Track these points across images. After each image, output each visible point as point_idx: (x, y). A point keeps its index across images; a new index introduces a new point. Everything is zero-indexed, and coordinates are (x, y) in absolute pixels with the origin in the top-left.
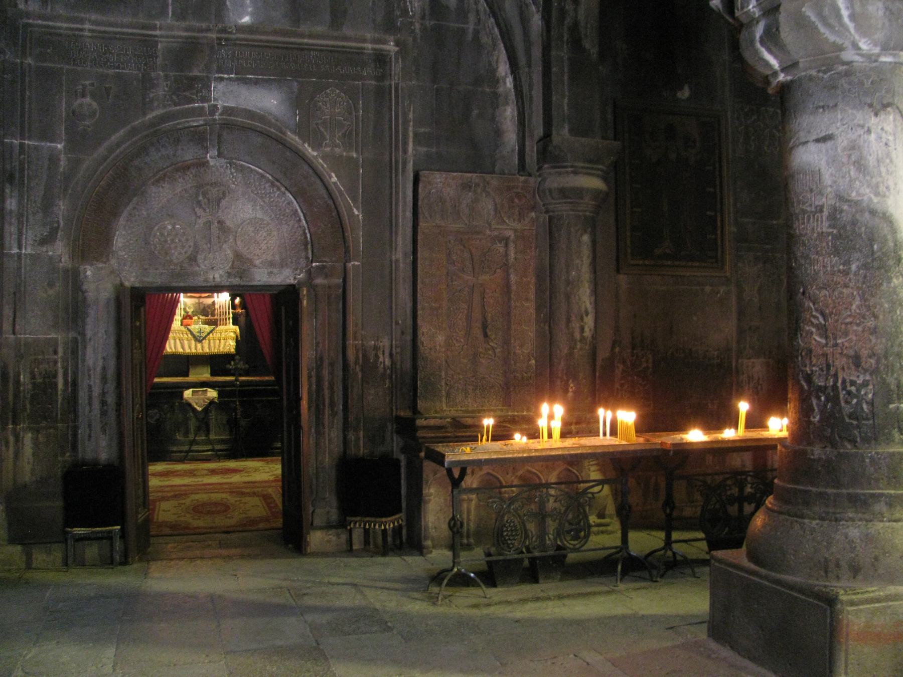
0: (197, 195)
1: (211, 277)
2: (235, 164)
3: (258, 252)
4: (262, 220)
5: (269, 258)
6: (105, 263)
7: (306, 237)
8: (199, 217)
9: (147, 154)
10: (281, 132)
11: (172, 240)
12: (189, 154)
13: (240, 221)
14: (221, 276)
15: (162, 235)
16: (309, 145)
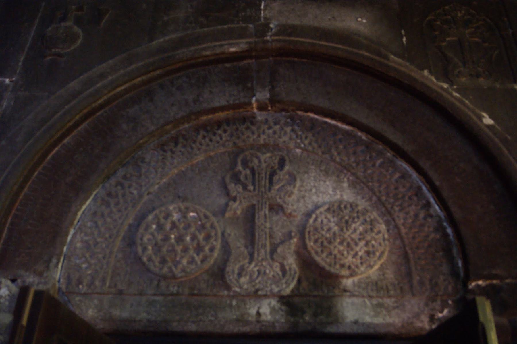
0: (234, 164)
1: (253, 311)
2: (301, 118)
3: (349, 260)
4: (353, 206)
5: (373, 272)
6: (40, 274)
7: (445, 235)
8: (234, 199)
9: (151, 100)
10: (379, 54)
11: (180, 239)
12: (219, 96)
13: (310, 207)
14: (273, 310)
15: (160, 227)
16: (431, 72)
